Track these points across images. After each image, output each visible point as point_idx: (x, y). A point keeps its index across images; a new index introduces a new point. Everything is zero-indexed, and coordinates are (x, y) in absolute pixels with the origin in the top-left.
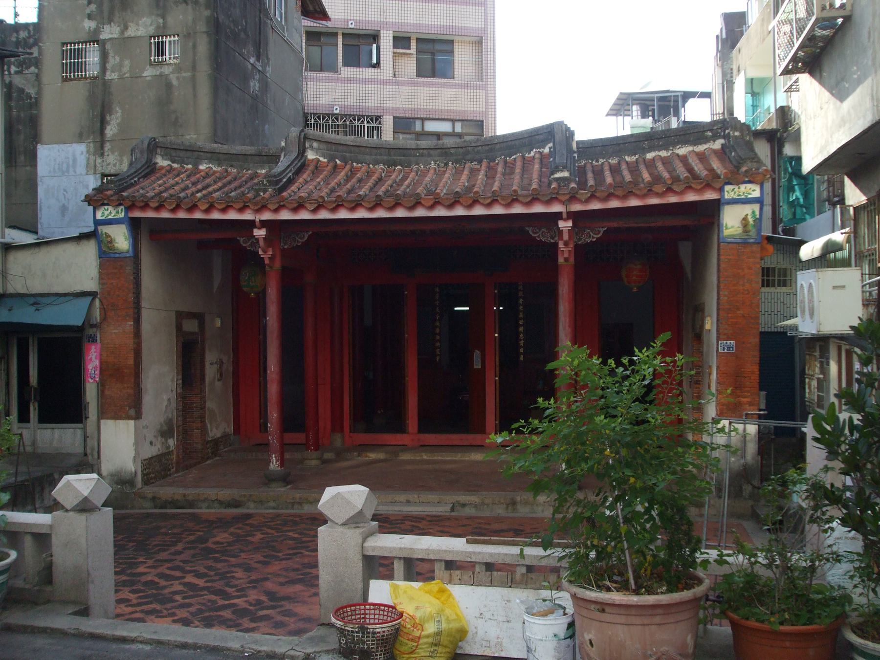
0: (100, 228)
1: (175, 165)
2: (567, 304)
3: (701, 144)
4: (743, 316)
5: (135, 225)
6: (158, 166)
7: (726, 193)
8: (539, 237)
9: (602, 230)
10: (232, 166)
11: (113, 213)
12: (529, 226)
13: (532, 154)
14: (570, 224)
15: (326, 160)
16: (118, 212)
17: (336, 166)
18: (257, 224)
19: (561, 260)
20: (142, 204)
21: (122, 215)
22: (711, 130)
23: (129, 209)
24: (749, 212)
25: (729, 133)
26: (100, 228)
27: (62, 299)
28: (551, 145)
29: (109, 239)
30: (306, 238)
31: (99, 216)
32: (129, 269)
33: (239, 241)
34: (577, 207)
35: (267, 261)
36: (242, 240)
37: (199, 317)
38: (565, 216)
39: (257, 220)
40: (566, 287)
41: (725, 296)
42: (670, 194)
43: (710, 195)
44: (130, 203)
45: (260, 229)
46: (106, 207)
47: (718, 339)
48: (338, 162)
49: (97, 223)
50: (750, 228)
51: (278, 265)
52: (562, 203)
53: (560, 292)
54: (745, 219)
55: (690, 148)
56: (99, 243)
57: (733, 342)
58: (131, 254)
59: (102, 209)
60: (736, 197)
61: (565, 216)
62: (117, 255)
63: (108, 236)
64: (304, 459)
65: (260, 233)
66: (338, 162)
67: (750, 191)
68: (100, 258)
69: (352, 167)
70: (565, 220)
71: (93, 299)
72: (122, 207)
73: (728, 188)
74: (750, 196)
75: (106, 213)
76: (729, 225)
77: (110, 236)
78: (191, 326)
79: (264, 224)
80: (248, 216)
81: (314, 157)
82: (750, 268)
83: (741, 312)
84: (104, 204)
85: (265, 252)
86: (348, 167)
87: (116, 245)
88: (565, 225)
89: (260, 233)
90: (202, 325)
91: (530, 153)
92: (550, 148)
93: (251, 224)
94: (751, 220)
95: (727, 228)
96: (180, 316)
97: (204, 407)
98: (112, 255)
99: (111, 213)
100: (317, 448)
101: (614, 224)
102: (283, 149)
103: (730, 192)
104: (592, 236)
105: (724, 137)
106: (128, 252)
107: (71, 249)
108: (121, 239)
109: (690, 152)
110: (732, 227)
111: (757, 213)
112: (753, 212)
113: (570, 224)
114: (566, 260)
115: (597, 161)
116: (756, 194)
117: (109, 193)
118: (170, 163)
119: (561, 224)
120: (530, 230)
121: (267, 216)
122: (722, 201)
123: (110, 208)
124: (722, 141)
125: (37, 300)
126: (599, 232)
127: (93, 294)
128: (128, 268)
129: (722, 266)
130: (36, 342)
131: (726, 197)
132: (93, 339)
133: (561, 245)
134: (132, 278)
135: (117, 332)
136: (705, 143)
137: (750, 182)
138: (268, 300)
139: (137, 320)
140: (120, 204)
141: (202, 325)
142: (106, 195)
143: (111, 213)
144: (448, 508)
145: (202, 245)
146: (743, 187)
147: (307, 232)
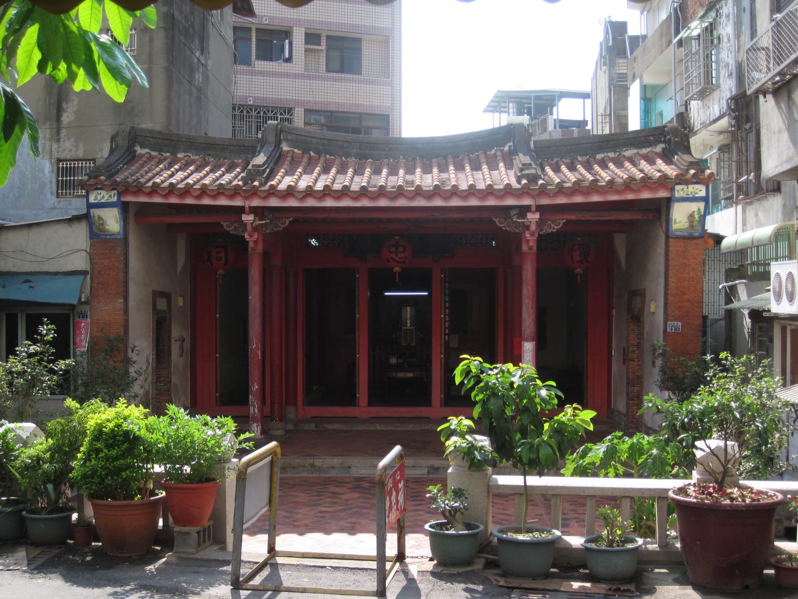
0: (92, 211)
1: (154, 153)
2: (530, 288)
3: (645, 147)
4: (688, 300)
5: (125, 208)
6: (137, 153)
7: (676, 192)
8: (505, 227)
9: (562, 222)
10: (209, 155)
11: (107, 197)
12: (496, 218)
13: (493, 151)
14: (537, 216)
15: (300, 152)
16: (110, 196)
17: (310, 158)
18: (247, 210)
19: (525, 248)
20: (135, 189)
21: (115, 199)
22: (652, 135)
23: (120, 194)
24: (696, 209)
25: (670, 138)
26: (92, 211)
27: (48, 277)
28: (511, 144)
29: (101, 222)
30: (287, 224)
31: (92, 199)
32: (119, 250)
33: (222, 225)
34: (545, 201)
35: (251, 245)
36: (225, 224)
37: (166, 296)
38: (533, 208)
39: (247, 206)
40: (530, 272)
41: (673, 282)
42: (628, 192)
43: (662, 194)
44: (124, 188)
45: (248, 214)
46: (99, 192)
47: (666, 320)
48: (312, 154)
49: (90, 206)
50: (695, 223)
51: (260, 249)
52: (532, 197)
53: (524, 277)
54: (691, 216)
55: (635, 151)
56: (90, 225)
57: (680, 324)
58: (122, 236)
59: (95, 192)
60: (685, 195)
61: (533, 208)
62: (108, 237)
63: (100, 218)
64: (269, 429)
65: (248, 218)
66: (312, 154)
67: (697, 191)
68: (91, 238)
69: (326, 159)
70: (533, 212)
71: (85, 278)
72: (115, 192)
73: (678, 187)
74: (697, 195)
75: (99, 197)
76: (678, 221)
77: (102, 219)
78: (162, 304)
79: (254, 210)
80: (238, 202)
81: (289, 149)
82: (695, 258)
83: (687, 297)
84: (97, 189)
85: (251, 236)
86: (322, 159)
87: (107, 227)
88: (533, 217)
89: (248, 218)
90: (169, 303)
91: (491, 150)
92: (510, 147)
93: (240, 210)
94: (697, 217)
95: (675, 223)
96: (156, 294)
97: (170, 382)
98: (103, 237)
99: (103, 197)
100: (281, 420)
101: (572, 217)
102: (259, 140)
103: (680, 191)
104: (553, 227)
105: (664, 142)
106: (119, 234)
107: (63, 229)
108: (112, 221)
109: (635, 154)
110: (680, 222)
111: (702, 210)
112: (699, 209)
113: (537, 216)
114: (530, 248)
115: (552, 160)
116: (703, 194)
117: (102, 178)
118: (149, 151)
119: (530, 216)
120: (497, 220)
121: (256, 203)
122: (673, 199)
123: (103, 192)
124: (663, 145)
125: (28, 277)
126: (560, 223)
127: (83, 273)
128: (119, 249)
129: (671, 256)
130: (24, 318)
131: (676, 195)
132: (84, 316)
133: (527, 235)
134: (122, 258)
135: (106, 310)
136: (648, 147)
137: (697, 183)
138: (250, 281)
139: (126, 298)
140: (114, 189)
141: (169, 303)
142: (100, 180)
143: (103, 197)
144: (425, 471)
145: (172, 228)
146: (691, 187)
147: (288, 218)
